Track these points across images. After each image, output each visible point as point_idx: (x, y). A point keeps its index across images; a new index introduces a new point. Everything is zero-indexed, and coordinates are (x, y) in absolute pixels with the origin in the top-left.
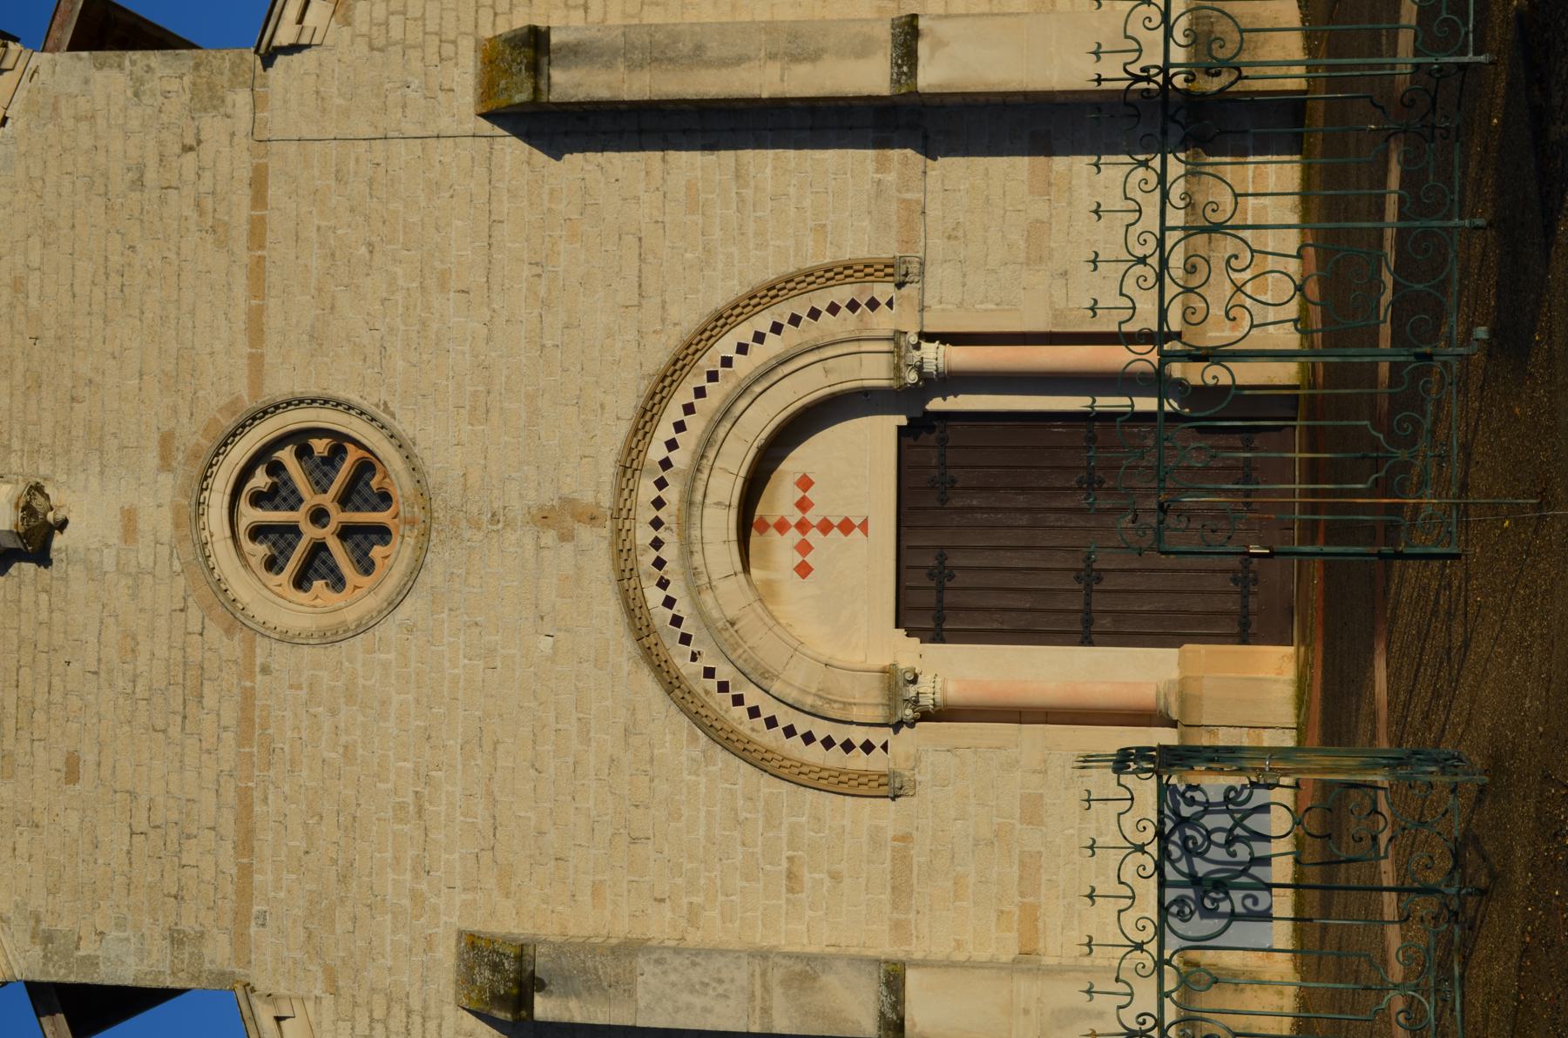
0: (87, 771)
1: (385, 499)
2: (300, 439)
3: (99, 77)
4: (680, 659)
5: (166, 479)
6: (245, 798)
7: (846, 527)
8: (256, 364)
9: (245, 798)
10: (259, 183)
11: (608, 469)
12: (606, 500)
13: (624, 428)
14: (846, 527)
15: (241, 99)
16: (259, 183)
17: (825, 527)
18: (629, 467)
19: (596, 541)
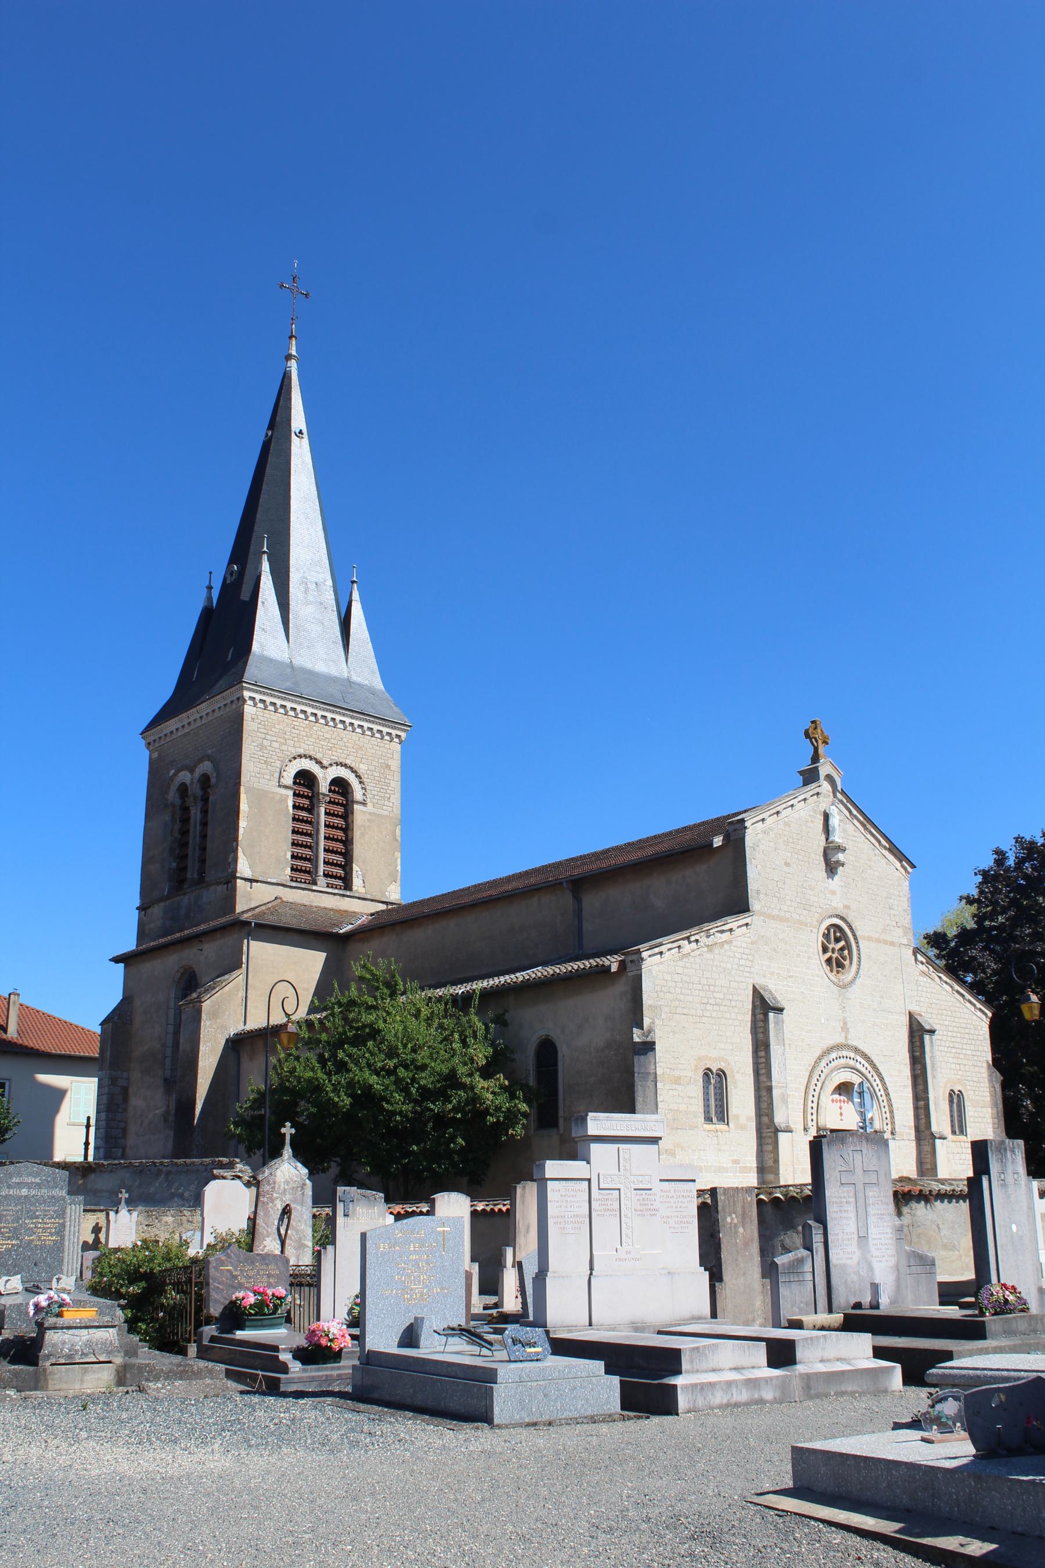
0: (786, 869)
1: (838, 972)
2: (848, 946)
3: (905, 899)
4: (823, 1063)
5: (841, 906)
6: (787, 920)
7: (841, 1114)
8: (870, 939)
9: (787, 920)
10: (892, 944)
11: (855, 1043)
12: (850, 1042)
13: (866, 1051)
14: (841, 1114)
15: (905, 941)
16: (892, 944)
17: (841, 1108)
18: (856, 1050)
19: (840, 1039)
